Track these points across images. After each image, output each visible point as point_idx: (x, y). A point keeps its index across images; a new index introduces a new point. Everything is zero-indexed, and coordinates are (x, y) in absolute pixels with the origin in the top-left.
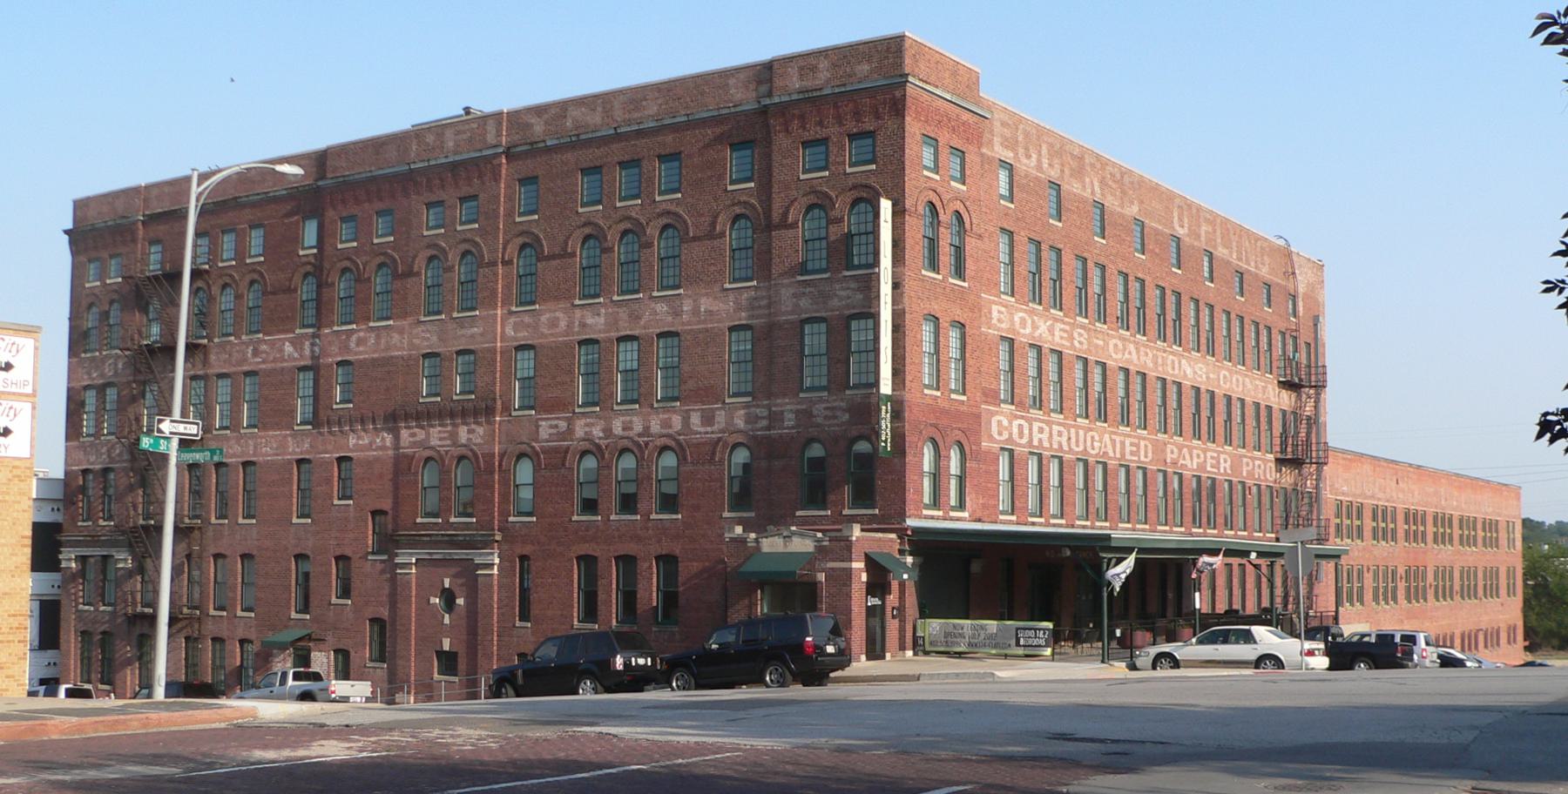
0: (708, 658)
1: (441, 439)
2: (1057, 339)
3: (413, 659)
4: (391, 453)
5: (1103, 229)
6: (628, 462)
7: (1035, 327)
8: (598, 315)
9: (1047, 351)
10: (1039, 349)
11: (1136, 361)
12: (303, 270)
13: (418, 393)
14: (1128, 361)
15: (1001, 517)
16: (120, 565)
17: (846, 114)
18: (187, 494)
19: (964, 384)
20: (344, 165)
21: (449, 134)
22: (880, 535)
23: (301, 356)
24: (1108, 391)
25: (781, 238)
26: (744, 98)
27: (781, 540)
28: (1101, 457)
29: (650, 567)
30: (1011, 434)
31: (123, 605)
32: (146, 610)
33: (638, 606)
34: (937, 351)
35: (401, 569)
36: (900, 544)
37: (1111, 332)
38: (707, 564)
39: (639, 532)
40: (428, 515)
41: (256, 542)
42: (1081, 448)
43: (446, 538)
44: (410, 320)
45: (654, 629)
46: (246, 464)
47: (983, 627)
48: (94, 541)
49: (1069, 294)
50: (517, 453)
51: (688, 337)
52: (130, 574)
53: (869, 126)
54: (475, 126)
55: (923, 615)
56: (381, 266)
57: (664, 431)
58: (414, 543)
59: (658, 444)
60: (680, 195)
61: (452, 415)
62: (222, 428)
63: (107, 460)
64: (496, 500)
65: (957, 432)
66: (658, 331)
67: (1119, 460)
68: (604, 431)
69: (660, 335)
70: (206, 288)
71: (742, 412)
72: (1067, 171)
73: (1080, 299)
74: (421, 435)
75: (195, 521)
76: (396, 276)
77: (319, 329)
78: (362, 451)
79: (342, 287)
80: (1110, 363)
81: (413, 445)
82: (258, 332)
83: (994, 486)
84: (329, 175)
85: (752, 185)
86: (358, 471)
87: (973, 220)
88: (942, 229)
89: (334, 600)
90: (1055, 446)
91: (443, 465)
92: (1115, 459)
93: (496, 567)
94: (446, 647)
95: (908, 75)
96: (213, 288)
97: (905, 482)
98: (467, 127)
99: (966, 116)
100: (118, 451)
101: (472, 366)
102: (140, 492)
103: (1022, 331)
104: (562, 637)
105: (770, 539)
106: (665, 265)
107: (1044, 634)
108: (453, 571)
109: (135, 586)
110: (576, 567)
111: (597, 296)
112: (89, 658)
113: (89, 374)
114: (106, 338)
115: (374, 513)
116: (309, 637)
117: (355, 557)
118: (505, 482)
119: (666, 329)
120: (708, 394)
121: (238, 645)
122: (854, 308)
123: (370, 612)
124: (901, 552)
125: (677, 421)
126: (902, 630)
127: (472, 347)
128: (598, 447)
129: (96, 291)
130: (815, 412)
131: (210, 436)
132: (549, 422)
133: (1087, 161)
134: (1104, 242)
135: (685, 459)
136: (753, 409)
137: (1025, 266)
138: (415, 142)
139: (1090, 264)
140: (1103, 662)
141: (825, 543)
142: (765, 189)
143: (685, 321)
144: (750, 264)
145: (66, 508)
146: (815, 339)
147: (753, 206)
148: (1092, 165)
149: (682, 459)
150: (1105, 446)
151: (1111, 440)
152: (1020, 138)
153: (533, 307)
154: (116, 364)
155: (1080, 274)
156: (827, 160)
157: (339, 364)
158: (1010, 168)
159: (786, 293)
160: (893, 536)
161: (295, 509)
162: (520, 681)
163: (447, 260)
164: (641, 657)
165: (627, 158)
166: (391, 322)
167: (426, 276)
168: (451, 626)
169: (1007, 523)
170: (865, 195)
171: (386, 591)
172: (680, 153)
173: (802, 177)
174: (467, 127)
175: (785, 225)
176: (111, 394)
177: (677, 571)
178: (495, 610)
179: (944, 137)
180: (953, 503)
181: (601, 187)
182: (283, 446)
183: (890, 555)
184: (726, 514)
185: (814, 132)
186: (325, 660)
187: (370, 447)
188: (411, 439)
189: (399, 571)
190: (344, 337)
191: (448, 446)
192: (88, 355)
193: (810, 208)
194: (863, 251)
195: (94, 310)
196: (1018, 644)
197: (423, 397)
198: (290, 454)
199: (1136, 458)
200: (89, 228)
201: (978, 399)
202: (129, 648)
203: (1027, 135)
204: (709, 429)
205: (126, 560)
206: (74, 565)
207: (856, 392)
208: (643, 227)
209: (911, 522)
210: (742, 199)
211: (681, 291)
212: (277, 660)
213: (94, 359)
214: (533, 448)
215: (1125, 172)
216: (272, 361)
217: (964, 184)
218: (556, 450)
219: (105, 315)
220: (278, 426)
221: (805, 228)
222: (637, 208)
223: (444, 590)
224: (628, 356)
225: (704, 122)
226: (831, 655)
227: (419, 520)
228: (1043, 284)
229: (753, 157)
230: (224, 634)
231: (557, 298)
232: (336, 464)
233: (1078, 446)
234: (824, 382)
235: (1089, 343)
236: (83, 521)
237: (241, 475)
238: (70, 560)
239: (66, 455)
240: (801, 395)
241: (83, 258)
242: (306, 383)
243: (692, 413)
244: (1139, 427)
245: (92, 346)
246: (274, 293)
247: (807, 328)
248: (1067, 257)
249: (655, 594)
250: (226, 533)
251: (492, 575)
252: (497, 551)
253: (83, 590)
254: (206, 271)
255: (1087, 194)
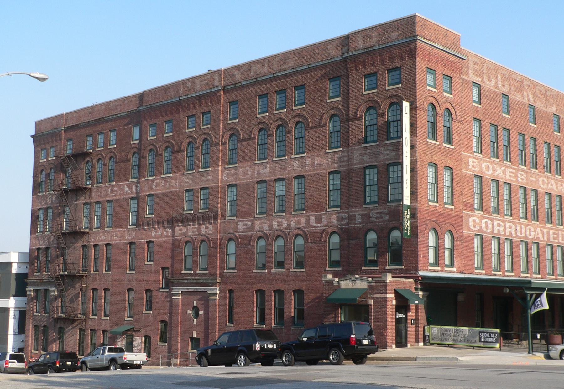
0: (301, 345)
1: (193, 232)
2: (508, 177)
3: (179, 341)
4: (171, 238)
5: (535, 119)
6: (280, 242)
7: (494, 170)
8: (266, 168)
9: (502, 183)
10: (497, 182)
11: (555, 189)
12: (133, 151)
13: (183, 209)
14: (551, 189)
15: (476, 271)
16: (52, 294)
17: (386, 59)
18: (81, 259)
19: (453, 200)
20: (151, 99)
21: (197, 81)
22: (403, 280)
23: (132, 192)
24: (539, 205)
25: (354, 126)
26: (335, 54)
27: (351, 282)
28: (535, 240)
29: (291, 296)
30: (481, 227)
31: (52, 313)
32: (63, 315)
33: (285, 316)
34: (436, 182)
35: (174, 296)
36: (416, 285)
37: (540, 174)
38: (318, 295)
39: (285, 278)
40: (187, 270)
41: (110, 283)
42: (523, 235)
43: (195, 281)
44: (180, 173)
45: (292, 328)
46: (107, 245)
47: (461, 331)
48: (41, 282)
49: (515, 153)
50: (228, 238)
51: (309, 178)
52: (56, 298)
53: (398, 65)
54: (209, 77)
55: (429, 323)
56: (167, 147)
57: (298, 226)
58: (180, 283)
59: (295, 233)
60: (304, 106)
61: (198, 220)
62: (97, 228)
63: (47, 243)
64: (218, 262)
65: (449, 225)
66: (294, 175)
67: (547, 242)
68: (268, 226)
69: (296, 178)
70: (91, 161)
71: (335, 216)
72: (513, 89)
73: (522, 156)
74: (184, 230)
75: (84, 273)
76: (174, 152)
77: (139, 179)
78: (158, 238)
79: (150, 158)
80: (539, 190)
81: (181, 234)
82: (113, 181)
83: (471, 254)
84: (144, 105)
85: (340, 99)
86: (156, 247)
87: (457, 113)
88: (438, 118)
89: (144, 311)
90: (508, 233)
91: (194, 244)
92: (544, 241)
93: (218, 295)
94: (195, 336)
95: (417, 35)
96: (94, 161)
97: (418, 252)
98: (205, 78)
99: (452, 58)
100: (52, 239)
101: (208, 195)
102: (62, 259)
103: (487, 172)
104: (232, 332)
105: (345, 281)
106: (298, 142)
107: (495, 336)
108: (199, 297)
109: (58, 304)
110: (255, 296)
111: (266, 159)
112: (38, 338)
113: (41, 203)
114: (48, 186)
115: (164, 268)
116: (132, 330)
117: (154, 290)
118: (222, 253)
119: (298, 174)
120: (319, 207)
121: (102, 333)
122: (391, 160)
123: (160, 318)
124: (416, 289)
125: (303, 221)
126: (417, 331)
127: (207, 186)
128: (266, 234)
129: (44, 164)
130: (372, 215)
131: (91, 231)
132: (243, 223)
133: (525, 83)
134: (535, 126)
135: (307, 240)
136: (341, 214)
137: (488, 137)
138: (182, 86)
139: (527, 138)
140: (529, 353)
141: (373, 284)
142: (346, 100)
143: (307, 170)
144: (339, 140)
145: (30, 266)
146: (371, 177)
147: (340, 110)
148: (528, 86)
149: (306, 241)
150: (538, 234)
151: (541, 230)
152: (485, 71)
153: (235, 165)
154: (52, 198)
155: (521, 143)
156: (377, 83)
157: (148, 196)
158: (479, 86)
159: (356, 154)
160: (412, 280)
161: (128, 266)
162: (210, 355)
163: (196, 143)
164: (270, 343)
165: (279, 89)
166: (171, 175)
167: (187, 152)
168: (197, 325)
169: (479, 274)
170: (396, 101)
171: (168, 307)
172: (305, 85)
173: (364, 93)
174: (205, 78)
175: (356, 118)
176: (50, 212)
177: (303, 298)
178: (217, 317)
179: (440, 69)
180: (447, 262)
181: (267, 104)
182: (123, 236)
183: (409, 291)
184: (327, 269)
185: (370, 69)
186: (140, 341)
187: (161, 236)
188: (180, 232)
189: (173, 297)
190: (150, 182)
191: (196, 235)
192: (41, 194)
193: (368, 109)
194: (396, 130)
195: (44, 172)
196: (480, 341)
197: (185, 211)
198: (126, 240)
199: (557, 241)
200: (42, 134)
201: (461, 208)
202: (54, 334)
203: (489, 69)
204: (319, 225)
205: (54, 291)
206: (32, 294)
207: (392, 204)
208: (287, 123)
209: (421, 273)
210: (335, 106)
211: (306, 154)
212: (119, 340)
213: (43, 196)
214: (235, 235)
215: (547, 89)
216: (119, 195)
217: (451, 94)
218: (246, 237)
219: (48, 175)
220: (121, 226)
221: (366, 120)
222: (284, 114)
223: (194, 307)
224: (280, 188)
225: (316, 68)
226: (366, 345)
227: (183, 272)
228: (499, 148)
229: (340, 84)
230: (96, 328)
231: (246, 161)
232: (146, 244)
233: (521, 234)
234: (376, 200)
235: (527, 179)
236: (37, 273)
237: (105, 250)
238: (31, 291)
239: (30, 241)
240: (364, 206)
241: (39, 149)
242: (133, 205)
243: (311, 217)
244: (558, 224)
245: (43, 190)
246: (120, 162)
247: (367, 172)
248: (514, 134)
249: (293, 310)
250: (98, 278)
251: (216, 299)
252: (218, 287)
253: (36, 306)
254: (91, 153)
255: (525, 101)
